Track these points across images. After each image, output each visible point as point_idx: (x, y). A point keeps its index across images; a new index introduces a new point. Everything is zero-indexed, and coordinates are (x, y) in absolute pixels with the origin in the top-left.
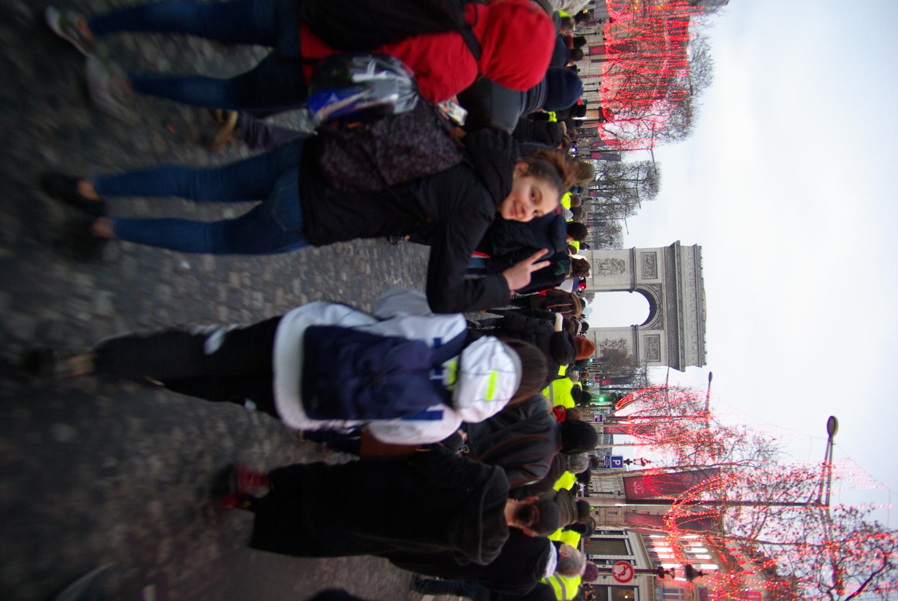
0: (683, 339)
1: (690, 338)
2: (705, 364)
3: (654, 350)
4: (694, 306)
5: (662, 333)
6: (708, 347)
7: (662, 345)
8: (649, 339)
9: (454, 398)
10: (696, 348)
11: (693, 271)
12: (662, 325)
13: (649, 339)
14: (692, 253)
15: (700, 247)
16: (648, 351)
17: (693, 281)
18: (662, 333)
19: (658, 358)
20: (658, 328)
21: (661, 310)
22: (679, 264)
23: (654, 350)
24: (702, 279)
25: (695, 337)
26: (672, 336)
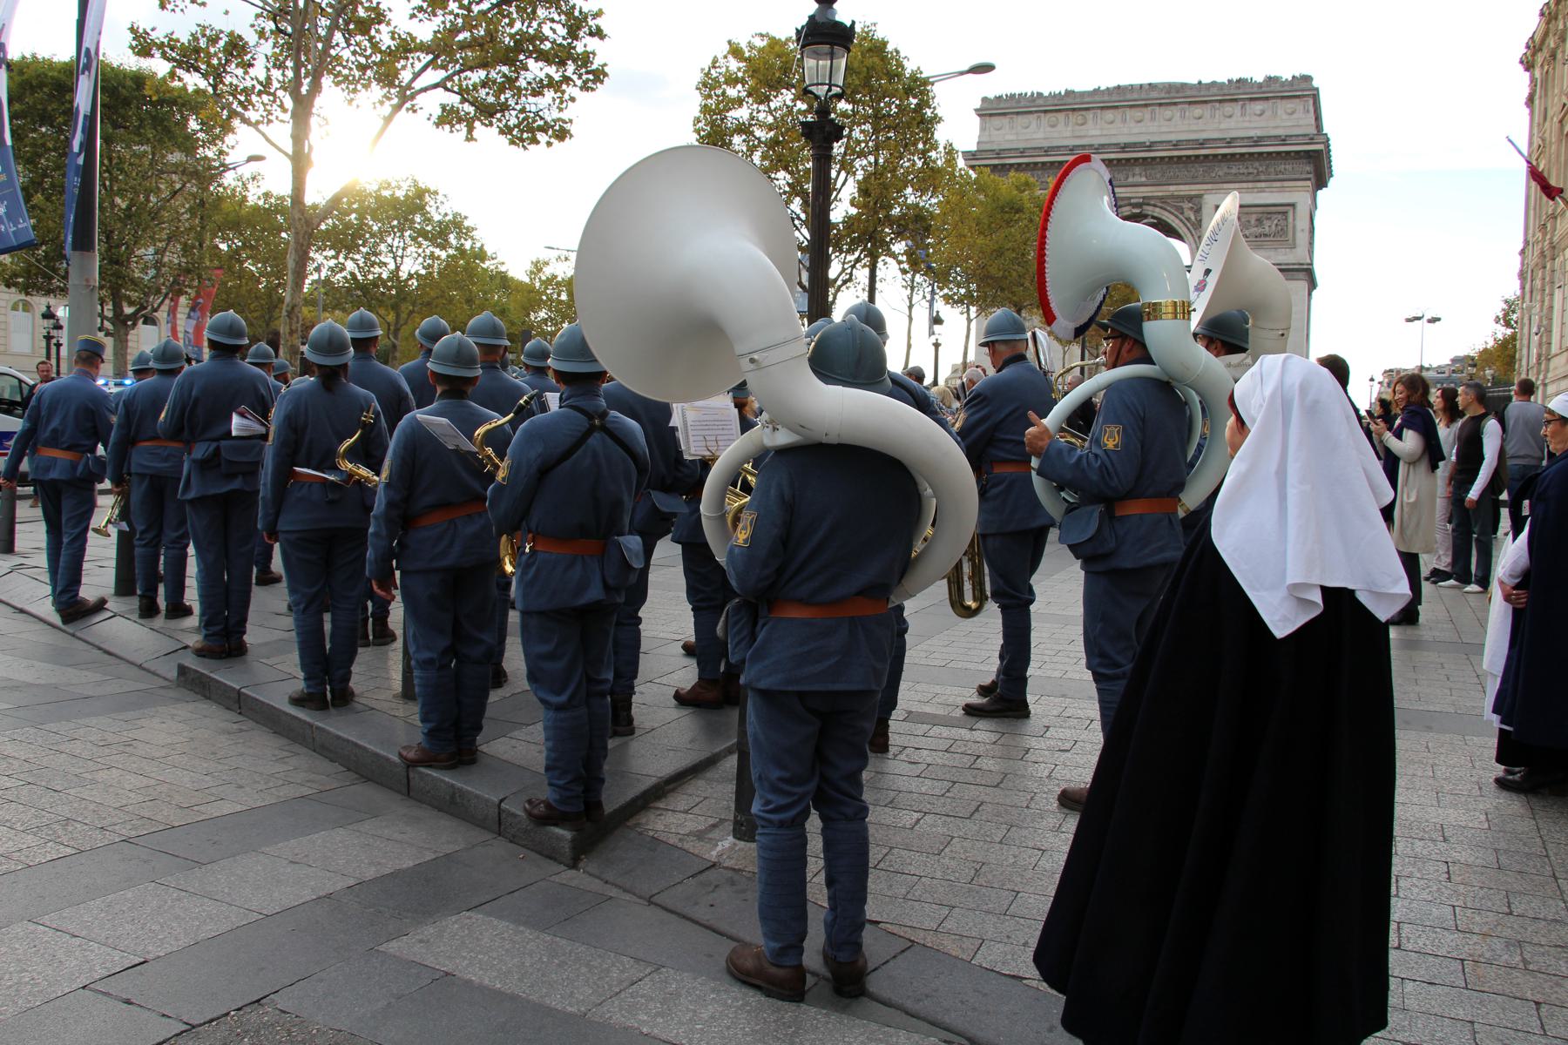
0: (1230, 142)
1: (1231, 123)
4: (1137, 113)
10: (1258, 107)
11: (1045, 119)
12: (1190, 198)
14: (997, 121)
15: (985, 100)
17: (1073, 117)
21: (1146, 201)
22: (1022, 152)
24: (1068, 93)
25: (1228, 108)
26: (1221, 170)
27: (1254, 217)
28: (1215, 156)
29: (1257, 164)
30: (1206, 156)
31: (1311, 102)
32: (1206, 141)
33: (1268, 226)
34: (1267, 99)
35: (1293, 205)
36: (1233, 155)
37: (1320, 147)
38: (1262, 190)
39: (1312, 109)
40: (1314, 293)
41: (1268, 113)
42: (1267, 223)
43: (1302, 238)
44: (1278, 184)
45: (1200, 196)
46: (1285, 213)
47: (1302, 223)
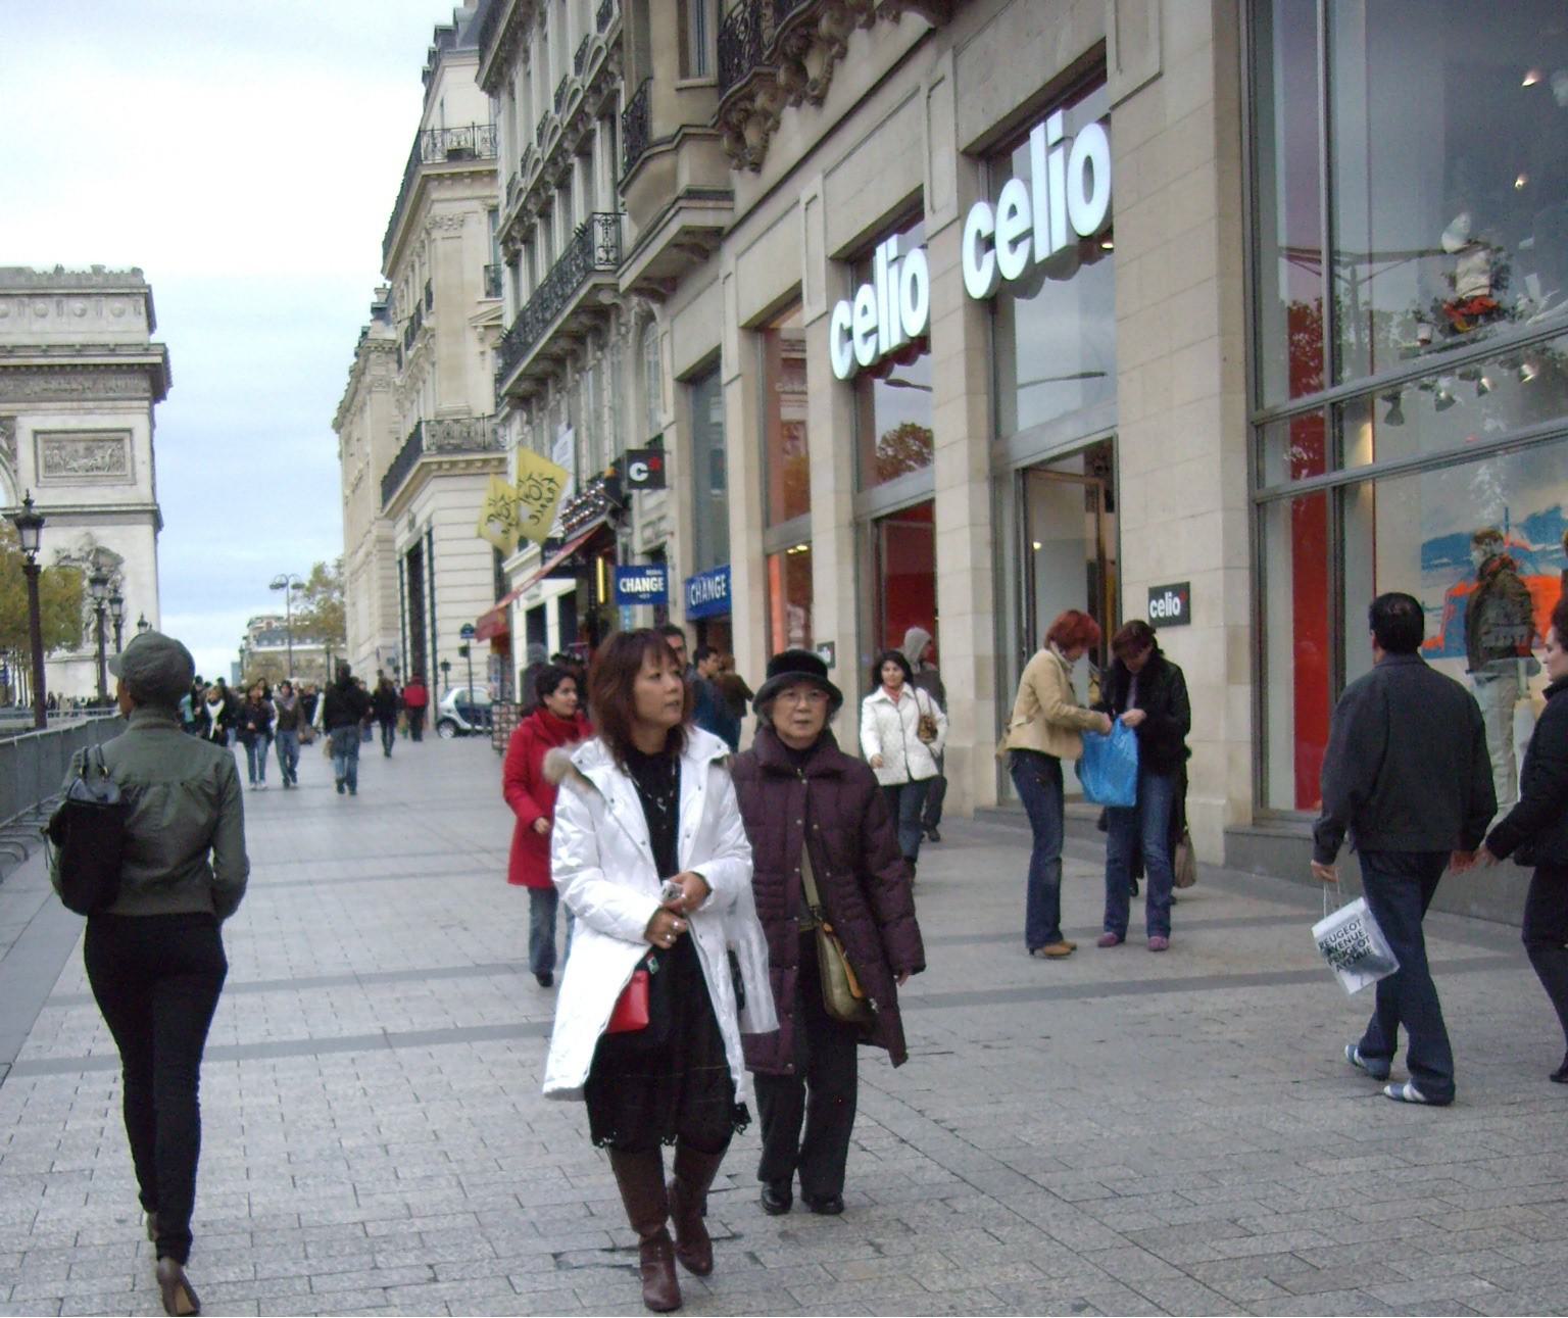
0: (47, 350)
1: (38, 325)
2: (137, 272)
3: (89, 452)
5: (29, 422)
6: (78, 261)
7: (72, 422)
8: (51, 468)
9: (672, 725)
10: (77, 305)
13: (51, 468)
16: (91, 475)
18: (29, 422)
19: (121, 435)
20: (11, 437)
23: (89, 452)
25: (40, 305)
26: (36, 384)
27: (81, 447)
28: (28, 367)
29: (80, 378)
30: (17, 367)
31: (142, 302)
32: (16, 347)
33: (102, 456)
34: (89, 295)
35: (129, 431)
36: (51, 366)
37: (158, 360)
38: (89, 411)
39: (143, 309)
40: (161, 535)
41: (91, 313)
42: (99, 454)
43: (143, 471)
44: (109, 404)
45: (12, 418)
46: (120, 440)
47: (141, 454)
